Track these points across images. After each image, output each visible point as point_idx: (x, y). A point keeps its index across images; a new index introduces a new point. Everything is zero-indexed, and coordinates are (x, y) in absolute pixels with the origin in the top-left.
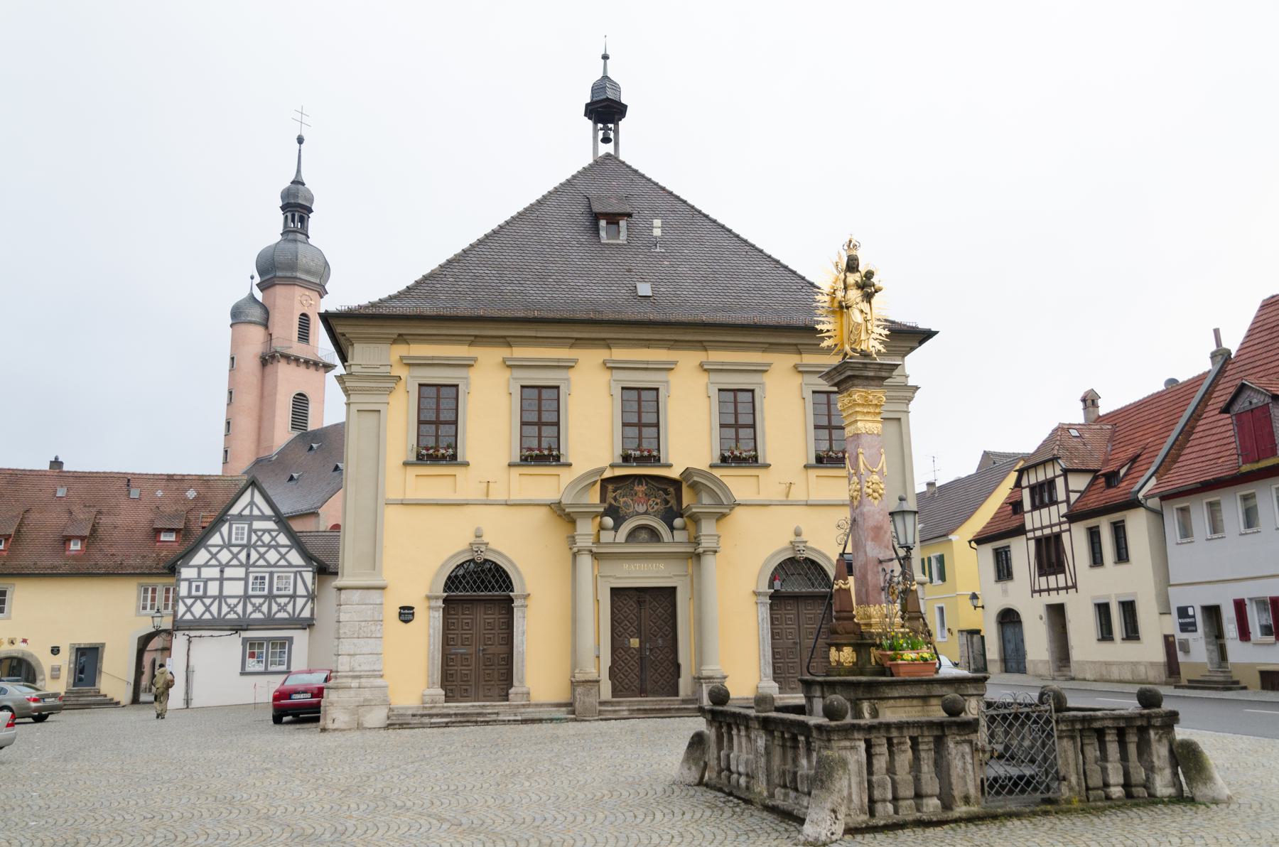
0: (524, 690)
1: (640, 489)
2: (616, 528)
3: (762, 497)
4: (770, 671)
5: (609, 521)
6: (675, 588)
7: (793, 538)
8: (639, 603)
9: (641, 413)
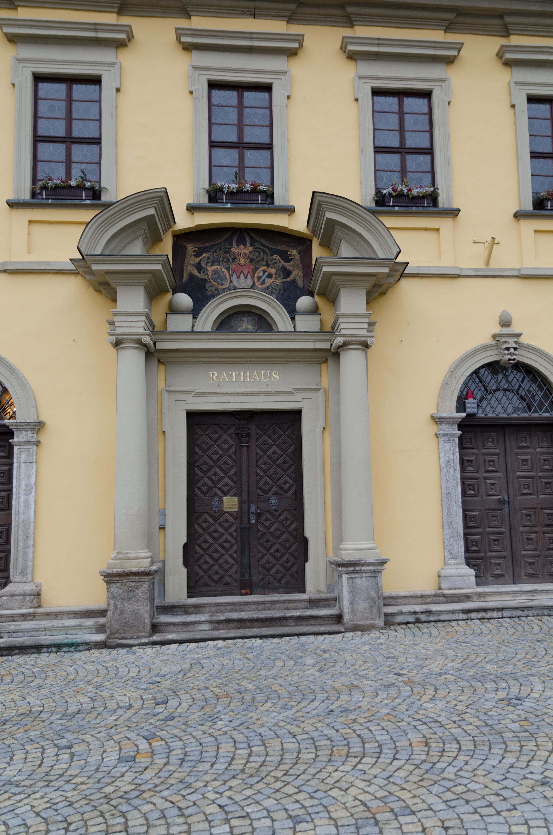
0: (29, 588)
1: (243, 251)
2: (195, 312)
3: (446, 263)
4: (460, 548)
5: (184, 300)
6: (298, 412)
7: (498, 330)
8: (239, 437)
9: (241, 124)
